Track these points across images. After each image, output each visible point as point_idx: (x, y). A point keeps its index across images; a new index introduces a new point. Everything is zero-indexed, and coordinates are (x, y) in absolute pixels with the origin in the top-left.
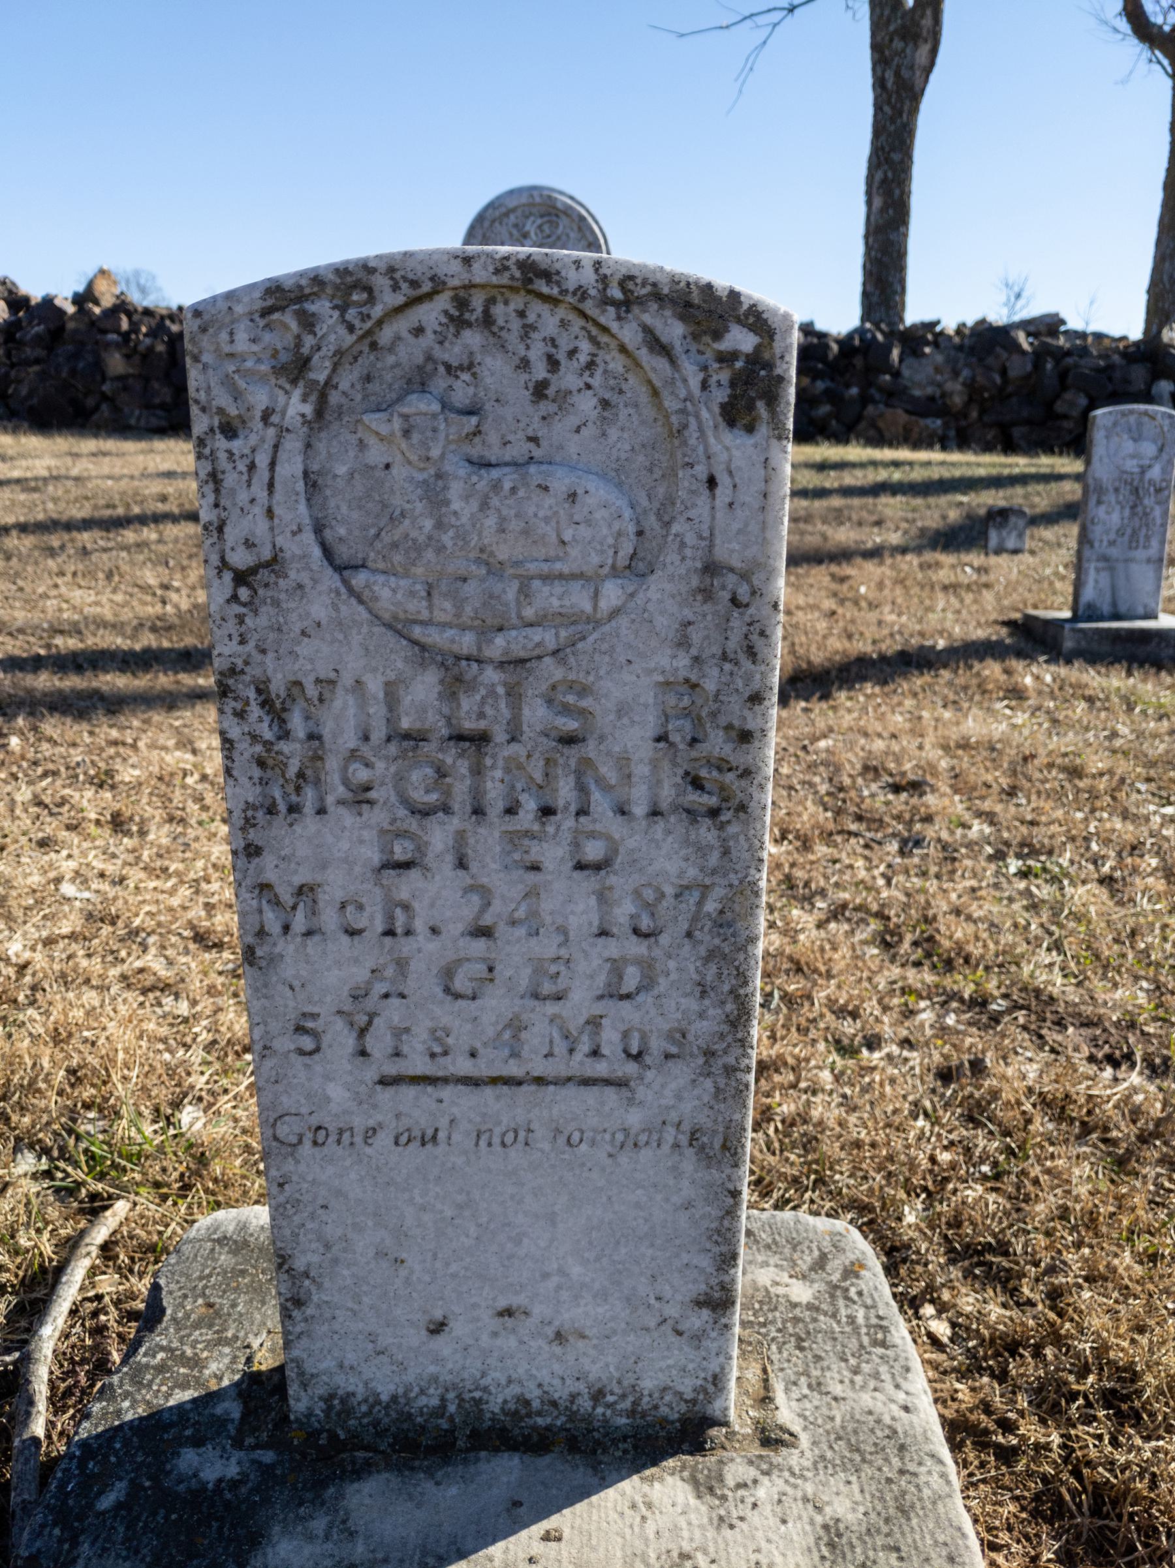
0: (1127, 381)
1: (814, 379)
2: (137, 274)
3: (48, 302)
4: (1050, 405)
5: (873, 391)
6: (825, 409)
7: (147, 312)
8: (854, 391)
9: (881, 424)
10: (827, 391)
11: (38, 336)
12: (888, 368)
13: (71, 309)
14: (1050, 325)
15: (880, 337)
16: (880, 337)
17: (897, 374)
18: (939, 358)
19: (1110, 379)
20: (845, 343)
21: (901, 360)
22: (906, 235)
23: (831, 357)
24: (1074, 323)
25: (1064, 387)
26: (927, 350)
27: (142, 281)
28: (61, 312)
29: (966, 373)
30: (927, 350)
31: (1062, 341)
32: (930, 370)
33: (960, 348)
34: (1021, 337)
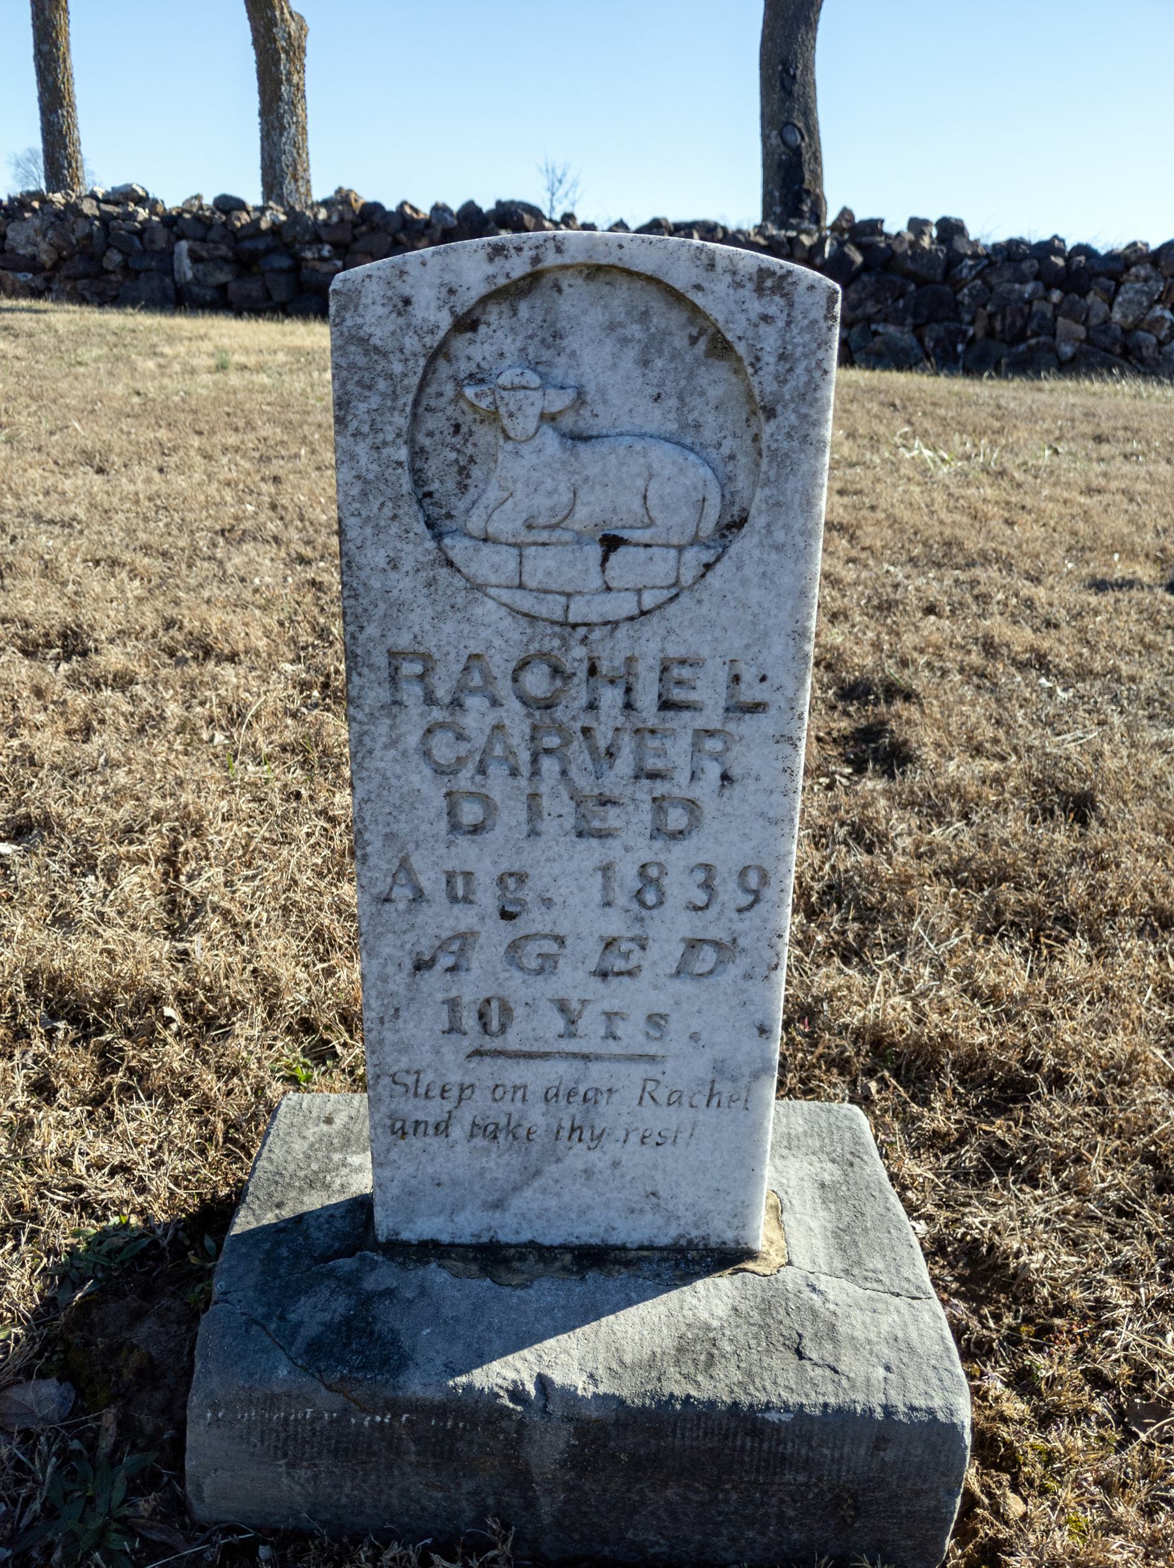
0: (152, 241)
26: (27, 215)
30: (27, 215)
32: (31, 232)
33: (58, 215)
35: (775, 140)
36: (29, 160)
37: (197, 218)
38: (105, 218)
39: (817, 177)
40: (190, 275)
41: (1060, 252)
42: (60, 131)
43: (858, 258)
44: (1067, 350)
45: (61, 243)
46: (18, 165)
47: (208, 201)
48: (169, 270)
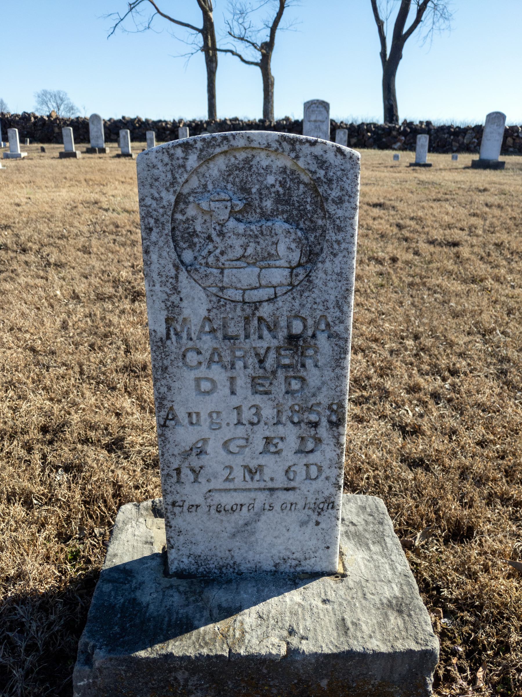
2: (59, 92)
3: (42, 117)
7: (63, 119)
11: (40, 125)
13: (47, 119)
14: (236, 119)
27: (61, 96)
28: (45, 120)
35: (387, 103)
36: (43, 94)
37: (256, 124)
38: (232, 124)
39: (397, 111)
41: (453, 128)
43: (409, 130)
44: (455, 149)
46: (39, 97)
47: (257, 121)
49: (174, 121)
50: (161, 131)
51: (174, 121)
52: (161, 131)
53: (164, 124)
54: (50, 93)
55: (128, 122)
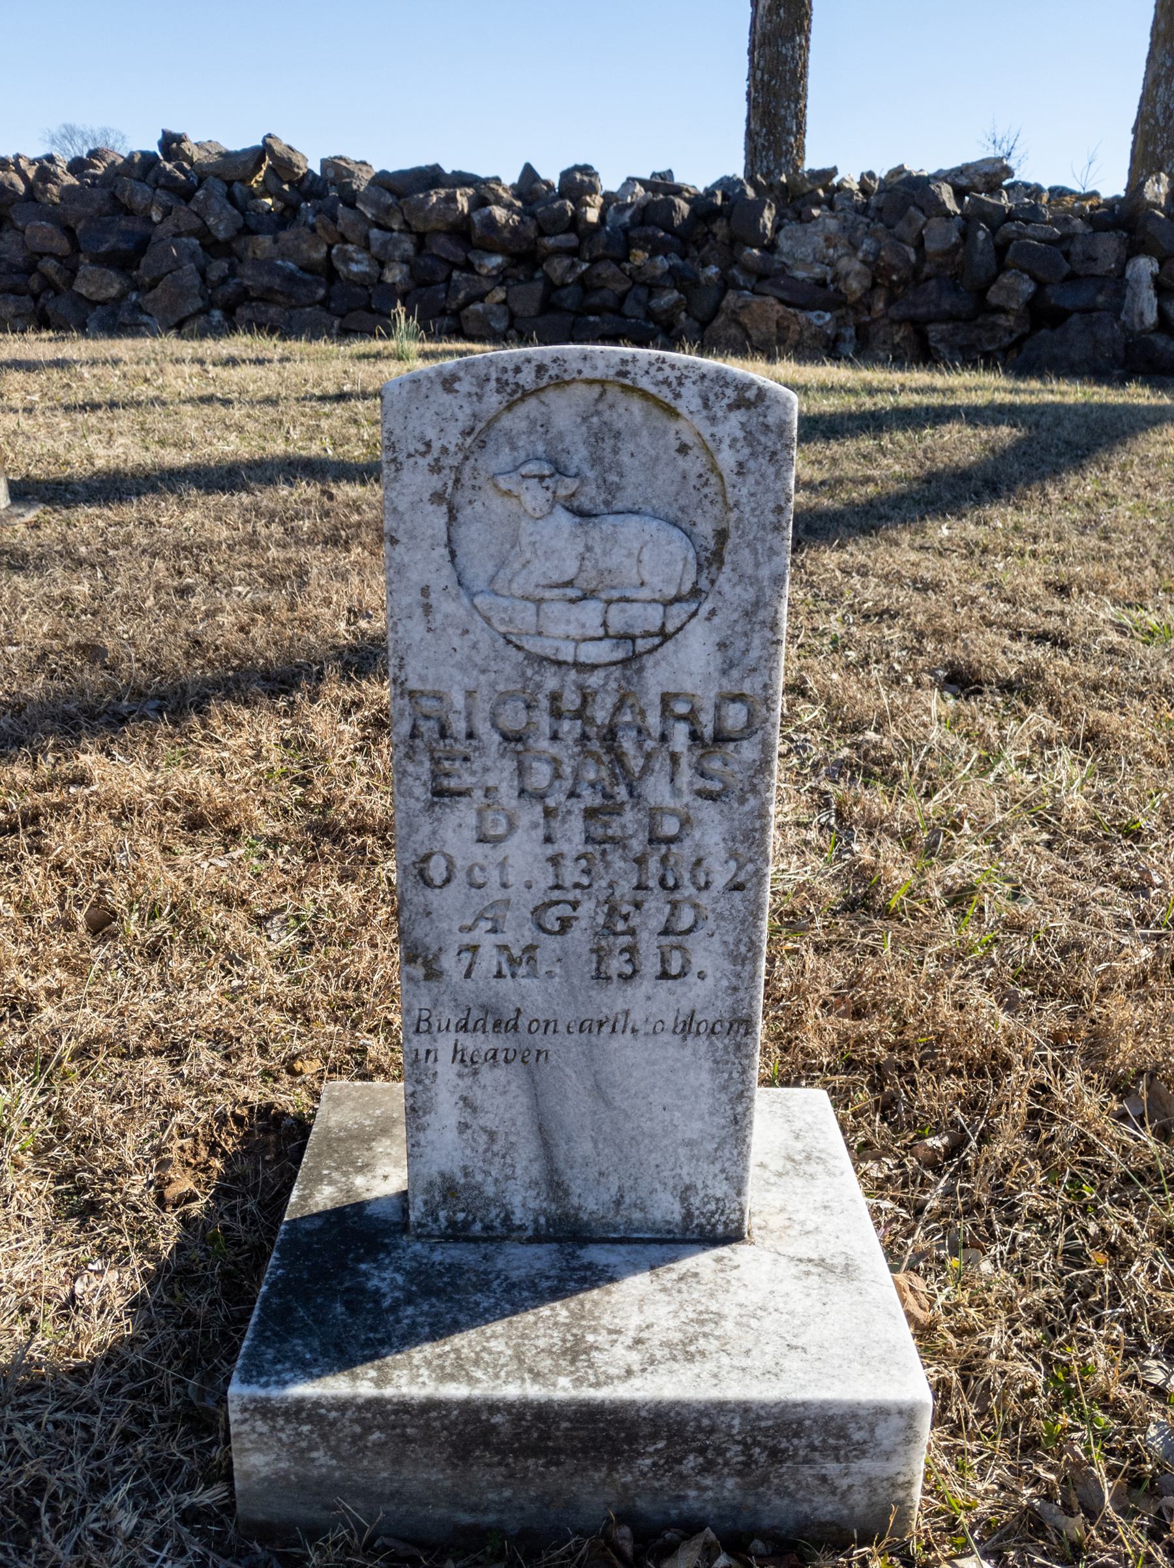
1: (653, 254)
4: (982, 292)
5: (735, 271)
6: (669, 297)
8: (712, 271)
9: (745, 319)
10: (672, 271)
12: (757, 239)
15: (750, 192)
16: (750, 192)
17: (771, 248)
18: (832, 224)
19: (1067, 255)
20: (702, 205)
21: (777, 228)
22: (805, 48)
23: (677, 222)
24: (1027, 172)
25: (1002, 268)
26: (816, 212)
29: (867, 245)
30: (816, 212)
31: (1004, 201)
32: (820, 241)
33: (863, 210)
34: (946, 194)
36: (64, 136)
40: (1151, 317)
42: (794, 72)
45: (895, 261)
48: (1117, 310)
49: (529, 172)
50: (442, 246)
51: (529, 172)
52: (442, 246)
53: (463, 202)
54: (82, 134)
55: (202, 175)
